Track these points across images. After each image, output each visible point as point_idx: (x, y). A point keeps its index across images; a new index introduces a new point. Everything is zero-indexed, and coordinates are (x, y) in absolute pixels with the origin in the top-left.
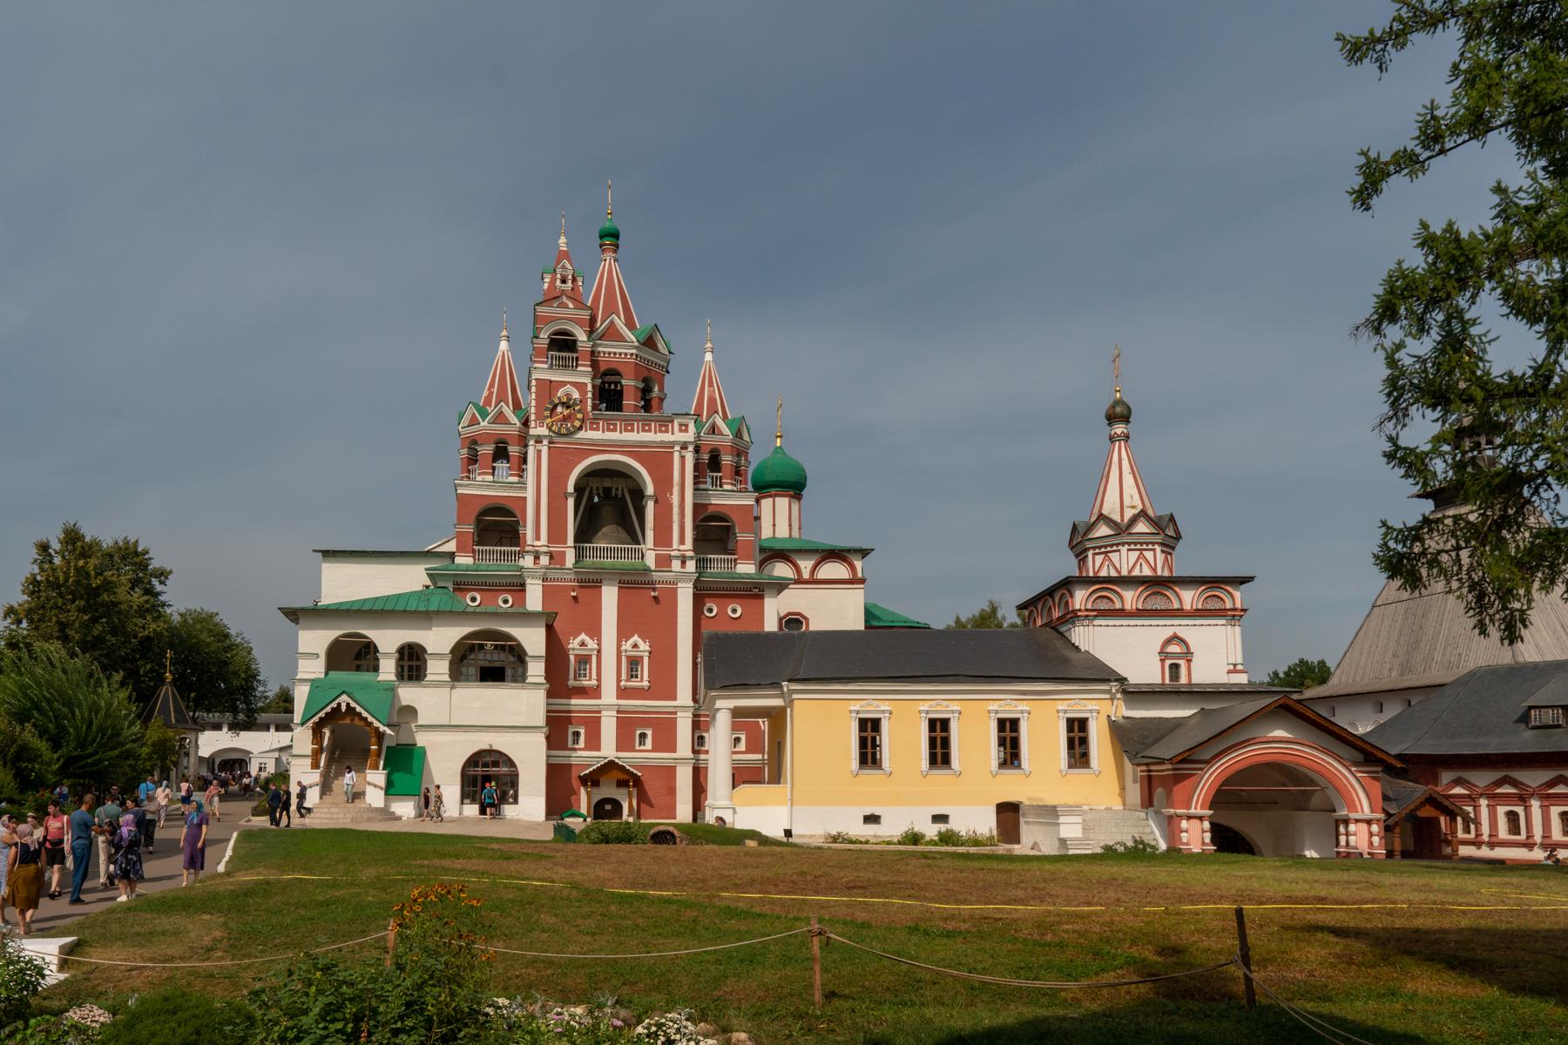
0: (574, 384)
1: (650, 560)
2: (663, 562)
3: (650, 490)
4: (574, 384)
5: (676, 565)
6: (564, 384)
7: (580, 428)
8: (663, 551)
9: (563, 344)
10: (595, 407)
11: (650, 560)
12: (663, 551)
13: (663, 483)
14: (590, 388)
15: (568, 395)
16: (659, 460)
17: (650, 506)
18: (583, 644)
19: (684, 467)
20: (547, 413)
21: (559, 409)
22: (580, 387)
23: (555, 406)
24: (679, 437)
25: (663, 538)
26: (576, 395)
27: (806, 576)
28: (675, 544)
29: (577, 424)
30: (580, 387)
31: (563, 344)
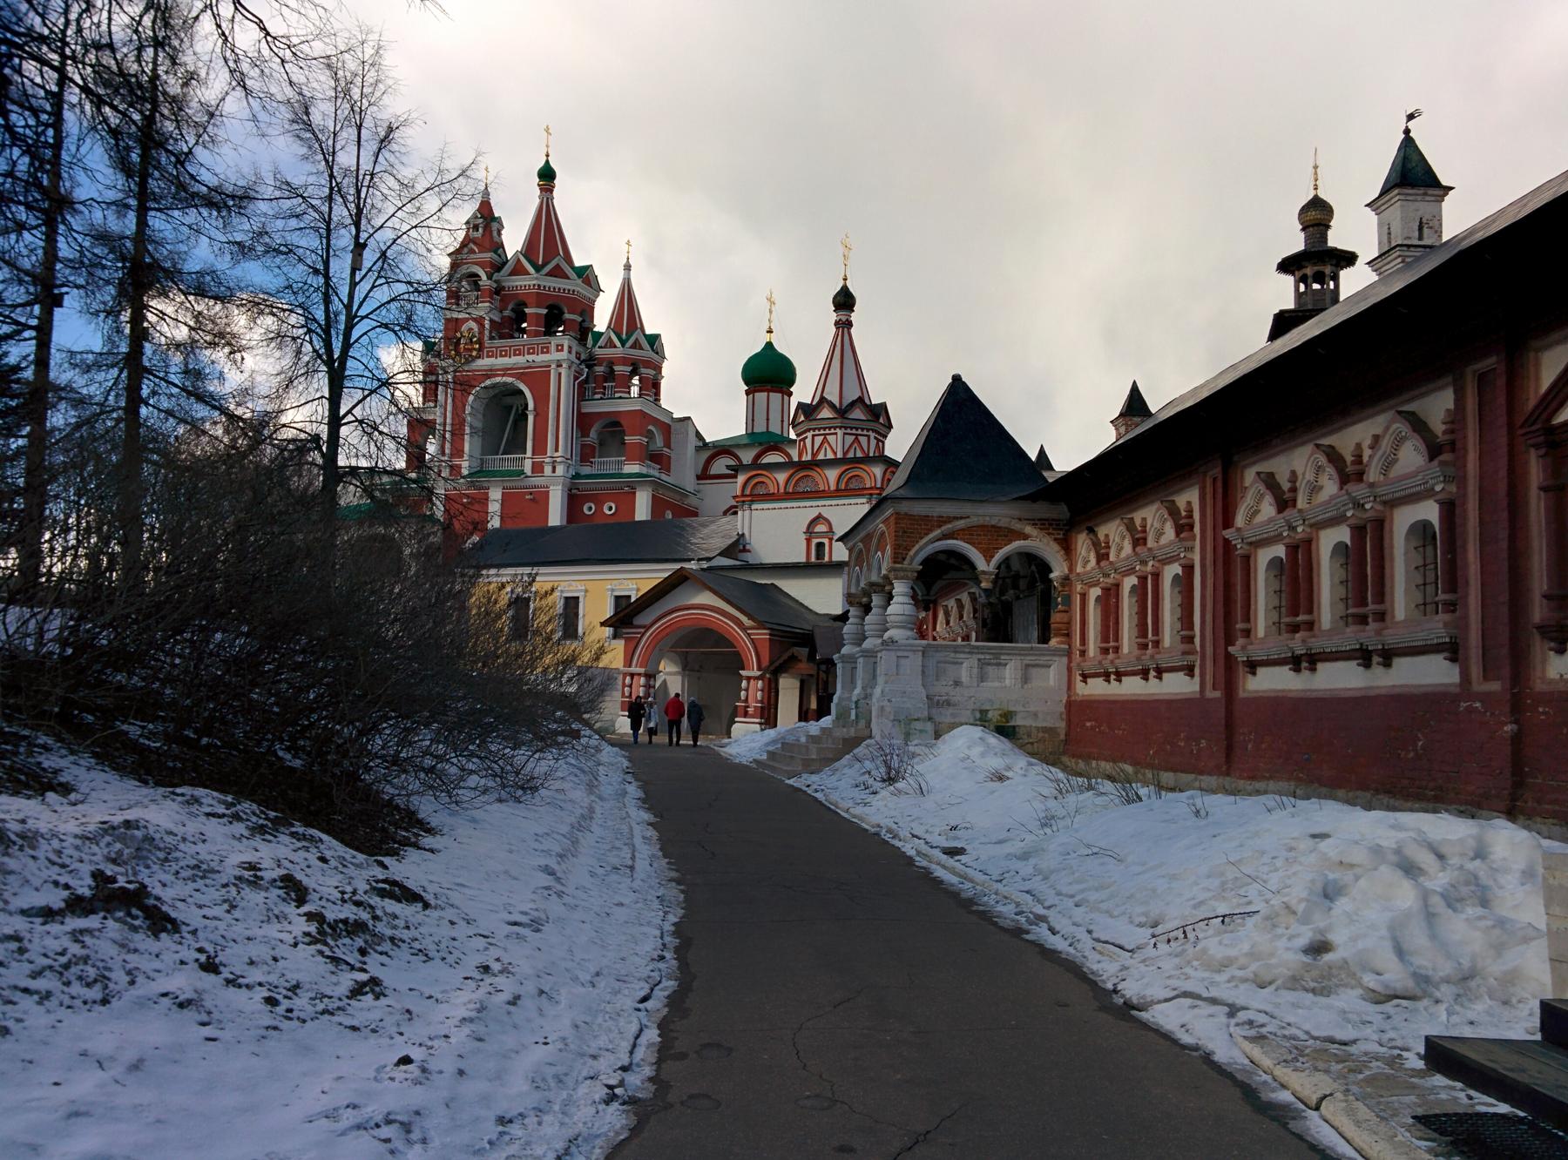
0: (474, 320)
2: (538, 468)
3: (531, 406)
5: (548, 470)
6: (467, 320)
8: (538, 459)
10: (491, 338)
11: (528, 468)
12: (538, 459)
13: (542, 398)
15: (470, 329)
16: (539, 379)
17: (531, 419)
22: (479, 321)
24: (555, 356)
25: (540, 448)
30: (479, 321)
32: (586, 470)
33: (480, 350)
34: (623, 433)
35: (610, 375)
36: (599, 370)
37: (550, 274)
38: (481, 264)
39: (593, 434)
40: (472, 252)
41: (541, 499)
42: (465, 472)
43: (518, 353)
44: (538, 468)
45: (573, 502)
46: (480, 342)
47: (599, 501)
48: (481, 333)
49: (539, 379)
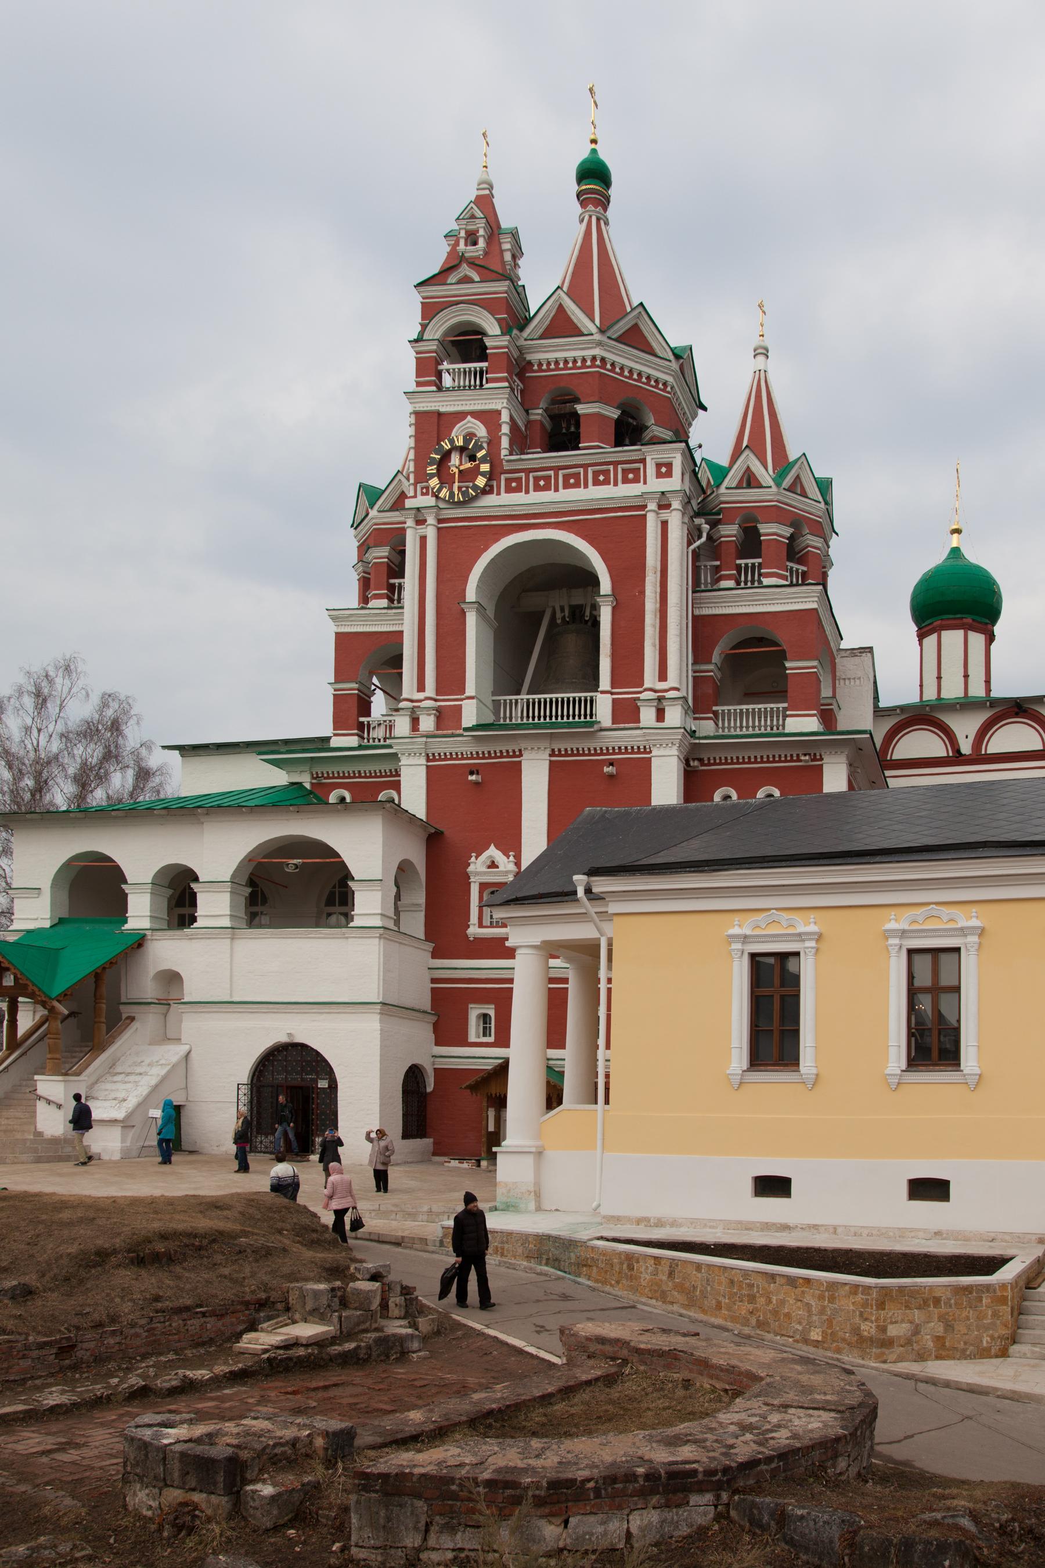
1: (603, 709)
3: (606, 585)
4: (477, 415)
5: (647, 715)
6: (461, 416)
7: (487, 491)
8: (626, 693)
9: (467, 345)
11: (603, 709)
12: (626, 693)
14: (505, 417)
15: (469, 436)
18: (493, 865)
19: (669, 545)
20: (432, 469)
21: (455, 459)
23: (446, 456)
25: (628, 671)
26: (481, 431)
27: (966, 748)
28: (650, 677)
29: (481, 482)
30: (489, 418)
31: (467, 345)
32: (707, 727)
33: (491, 476)
34: (782, 656)
35: (750, 542)
36: (730, 531)
37: (618, 340)
38: (488, 305)
39: (716, 657)
40: (466, 280)
41: (637, 771)
42: (470, 715)
43: (573, 481)
44: (626, 713)
45: (696, 780)
46: (493, 458)
47: (746, 781)
48: (494, 442)
49: (619, 534)
